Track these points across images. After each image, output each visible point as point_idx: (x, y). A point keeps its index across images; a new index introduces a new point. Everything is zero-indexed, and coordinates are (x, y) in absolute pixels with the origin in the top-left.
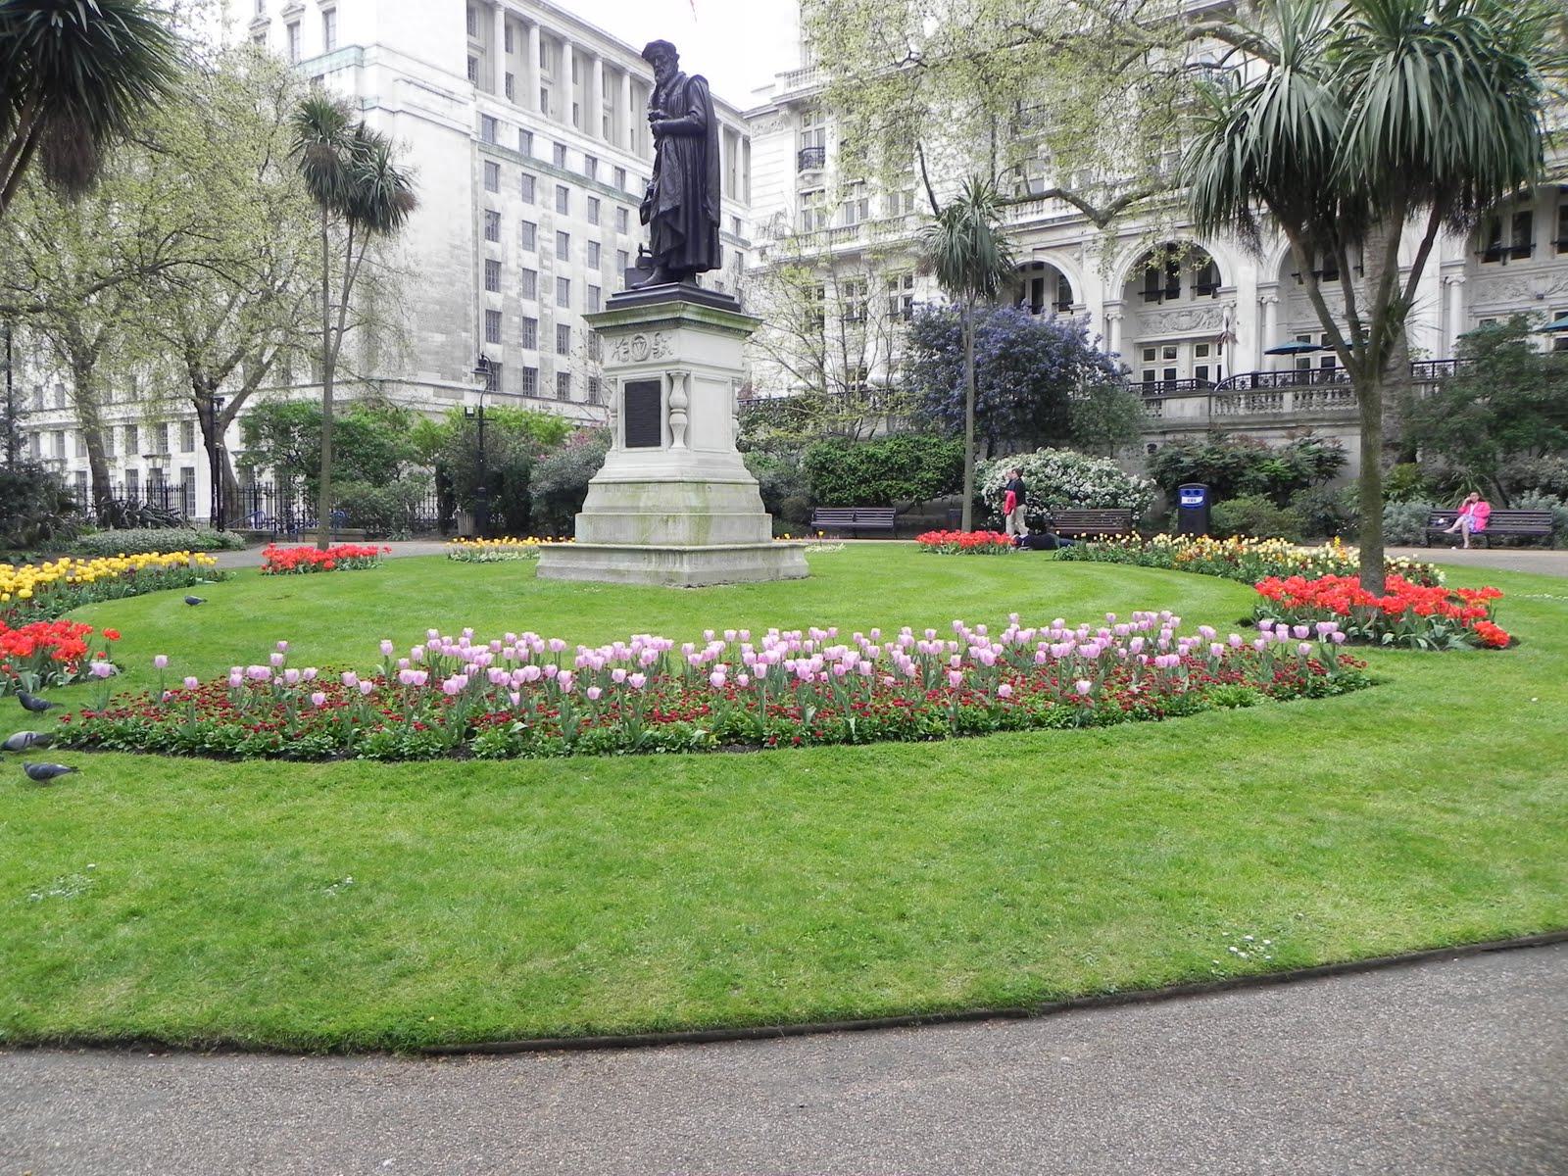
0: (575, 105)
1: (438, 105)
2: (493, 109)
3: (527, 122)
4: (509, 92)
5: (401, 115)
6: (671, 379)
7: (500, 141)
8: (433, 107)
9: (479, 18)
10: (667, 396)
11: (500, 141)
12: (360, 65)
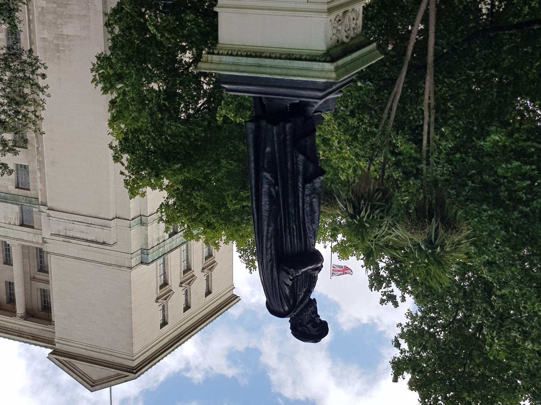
1: (78, 230)
4: (7, 249)
8: (83, 227)
9: (37, 303)
12: (144, 251)
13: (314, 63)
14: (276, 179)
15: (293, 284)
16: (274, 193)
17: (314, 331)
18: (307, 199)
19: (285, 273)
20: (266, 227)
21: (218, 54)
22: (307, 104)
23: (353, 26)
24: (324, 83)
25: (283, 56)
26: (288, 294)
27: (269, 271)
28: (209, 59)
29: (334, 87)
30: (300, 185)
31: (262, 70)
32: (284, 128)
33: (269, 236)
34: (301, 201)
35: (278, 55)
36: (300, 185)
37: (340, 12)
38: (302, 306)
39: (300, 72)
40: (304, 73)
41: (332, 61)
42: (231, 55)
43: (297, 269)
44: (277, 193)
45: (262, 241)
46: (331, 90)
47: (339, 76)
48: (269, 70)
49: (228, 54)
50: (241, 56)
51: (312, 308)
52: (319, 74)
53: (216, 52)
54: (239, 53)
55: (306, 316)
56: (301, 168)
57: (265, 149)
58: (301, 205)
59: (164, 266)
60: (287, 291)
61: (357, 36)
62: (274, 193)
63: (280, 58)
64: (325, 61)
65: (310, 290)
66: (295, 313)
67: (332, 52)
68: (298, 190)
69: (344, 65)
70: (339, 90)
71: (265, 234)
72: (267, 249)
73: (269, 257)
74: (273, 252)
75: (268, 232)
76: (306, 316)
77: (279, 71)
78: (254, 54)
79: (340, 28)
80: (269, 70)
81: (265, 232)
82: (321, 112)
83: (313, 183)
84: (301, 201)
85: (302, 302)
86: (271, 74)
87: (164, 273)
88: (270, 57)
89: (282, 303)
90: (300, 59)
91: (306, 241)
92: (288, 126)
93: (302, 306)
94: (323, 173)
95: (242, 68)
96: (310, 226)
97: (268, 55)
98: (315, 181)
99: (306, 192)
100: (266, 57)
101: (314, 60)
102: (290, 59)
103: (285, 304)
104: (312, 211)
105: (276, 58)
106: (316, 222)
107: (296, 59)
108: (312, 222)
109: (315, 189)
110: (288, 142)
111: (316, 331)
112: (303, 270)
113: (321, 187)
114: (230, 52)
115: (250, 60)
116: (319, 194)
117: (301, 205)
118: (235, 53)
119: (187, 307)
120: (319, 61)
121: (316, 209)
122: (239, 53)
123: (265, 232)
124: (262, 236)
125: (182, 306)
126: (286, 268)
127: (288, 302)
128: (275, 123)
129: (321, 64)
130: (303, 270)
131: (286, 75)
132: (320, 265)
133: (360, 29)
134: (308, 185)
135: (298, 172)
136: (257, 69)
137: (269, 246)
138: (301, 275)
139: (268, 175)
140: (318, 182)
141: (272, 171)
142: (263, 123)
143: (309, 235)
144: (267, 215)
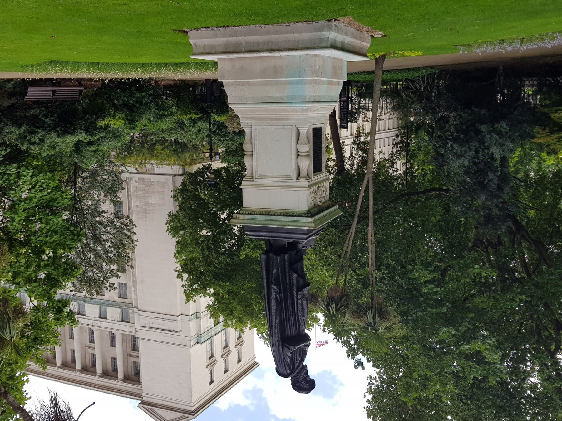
0: (72, 337)
2: (125, 327)
3: (103, 324)
5: (178, 315)
6: (308, 176)
7: (119, 310)
10: (306, 164)
11: (119, 310)
13: (301, 218)
14: (280, 289)
15: (292, 356)
16: (279, 298)
17: (306, 386)
18: (300, 301)
19: (286, 348)
20: (274, 320)
21: (243, 214)
22: (298, 242)
23: (324, 195)
24: (308, 230)
25: (282, 214)
26: (289, 362)
27: (277, 348)
28: (238, 217)
29: (314, 232)
30: (295, 292)
31: (270, 223)
32: (284, 257)
33: (277, 324)
34: (295, 303)
35: (279, 214)
36: (295, 292)
37: (316, 188)
38: (298, 370)
39: (293, 224)
40: (295, 224)
41: (312, 216)
42: (251, 214)
43: (294, 345)
44: (281, 298)
45: (272, 329)
46: (312, 233)
47: (316, 226)
48: (274, 223)
49: (248, 214)
50: (257, 214)
51: (305, 371)
52: (304, 224)
53: (241, 212)
54: (256, 213)
55: (301, 376)
56: (295, 282)
57: (273, 270)
58: (296, 305)
59: (211, 345)
60: (289, 360)
61: (327, 201)
62: (279, 298)
63: (280, 215)
64: (308, 217)
65: (303, 360)
66: (294, 375)
67: (311, 211)
68: (294, 296)
69: (319, 219)
70: (317, 233)
71: (274, 324)
72: (275, 334)
73: (277, 339)
74: (279, 336)
75: (276, 323)
76: (301, 376)
77: (280, 223)
78: (264, 213)
79: (316, 196)
80: (274, 223)
81: (274, 323)
82: (306, 247)
83: (303, 292)
84: (295, 303)
85: (298, 367)
86: (275, 225)
87: (212, 349)
88: (274, 215)
89: (285, 368)
90: (293, 216)
91: (299, 328)
92: (286, 256)
93: (298, 370)
94: (308, 285)
95: (257, 222)
96: (302, 318)
97: (273, 213)
98: (304, 290)
99: (299, 297)
100: (272, 215)
101: (301, 216)
102: (286, 216)
103: (287, 368)
104: (303, 309)
105: (278, 215)
106: (305, 315)
107: (290, 216)
108: (303, 316)
109: (304, 295)
110: (286, 266)
111: (308, 386)
112: (298, 346)
113: (308, 293)
114: (250, 212)
115: (262, 217)
116: (306, 298)
117: (296, 305)
118: (253, 213)
119: (226, 371)
120: (304, 217)
121: (305, 307)
122: (256, 213)
123: (274, 323)
124: (272, 326)
125: (223, 370)
126: (287, 345)
127: (290, 368)
128: (278, 255)
129: (305, 218)
130: (298, 346)
131: (284, 225)
132: (308, 343)
133: (328, 197)
134: (300, 293)
135: (293, 284)
136: (266, 222)
137: (276, 332)
138: (297, 350)
139: (275, 287)
140: (306, 290)
141: (278, 284)
142: (271, 255)
143: (301, 324)
144: (275, 312)
